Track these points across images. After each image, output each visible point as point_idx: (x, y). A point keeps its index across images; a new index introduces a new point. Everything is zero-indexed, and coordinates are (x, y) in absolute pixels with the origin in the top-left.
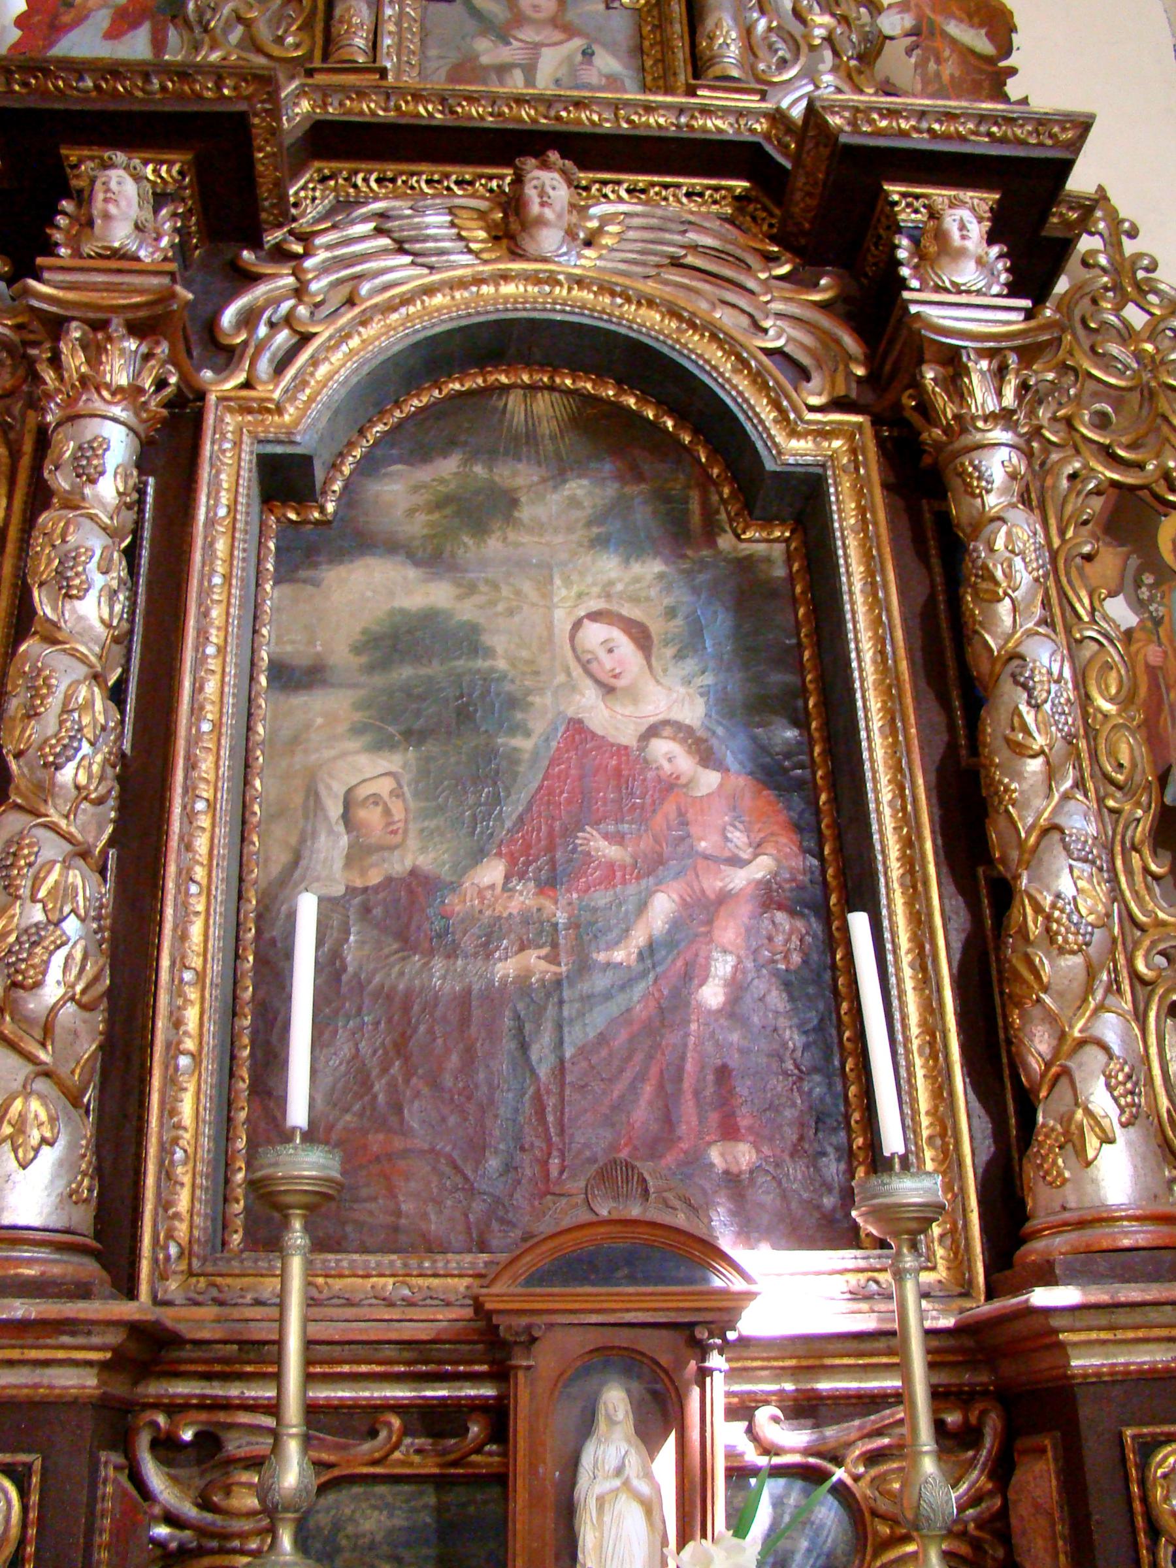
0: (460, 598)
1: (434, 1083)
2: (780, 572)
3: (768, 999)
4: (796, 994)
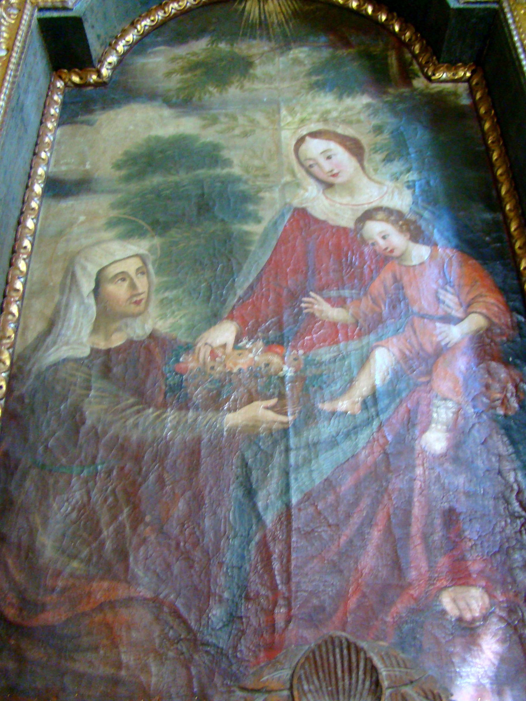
0: (204, 127)
1: (161, 530)
2: (465, 101)
3: (490, 442)
4: (517, 436)
